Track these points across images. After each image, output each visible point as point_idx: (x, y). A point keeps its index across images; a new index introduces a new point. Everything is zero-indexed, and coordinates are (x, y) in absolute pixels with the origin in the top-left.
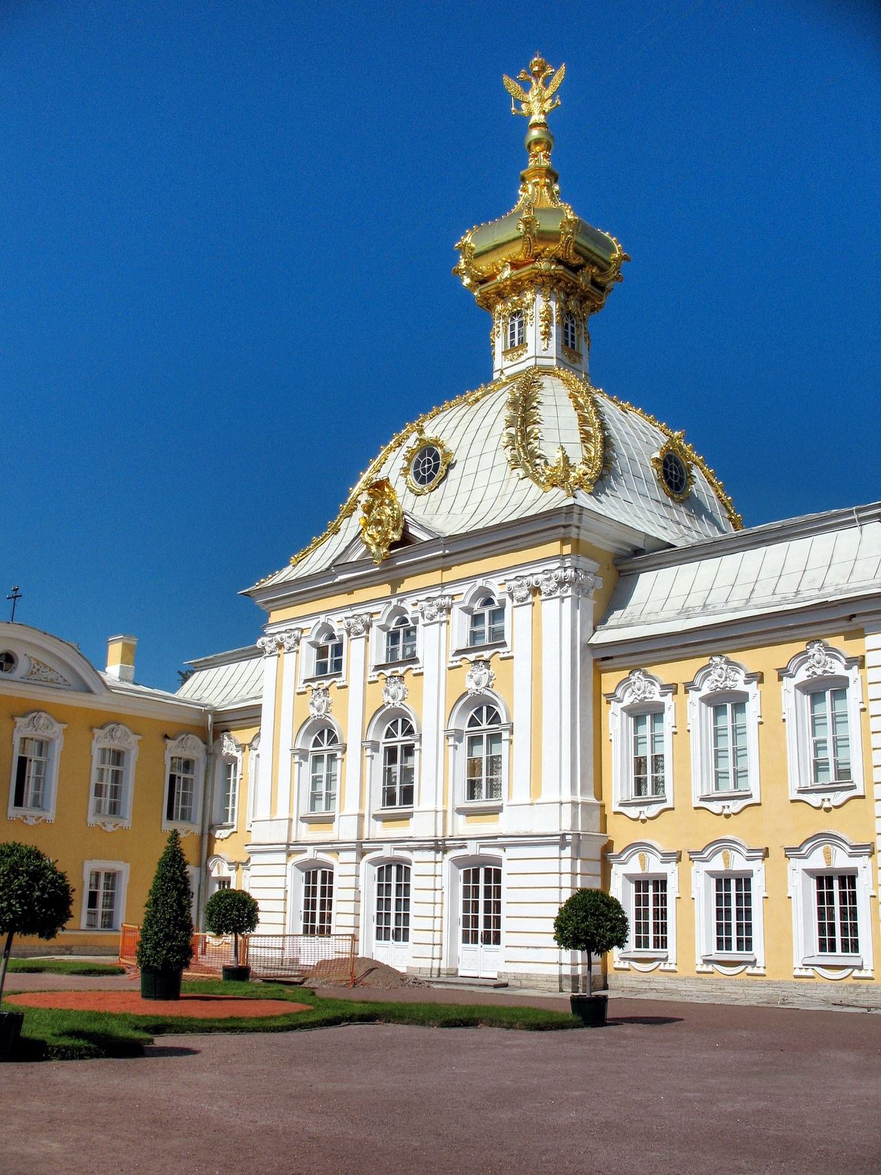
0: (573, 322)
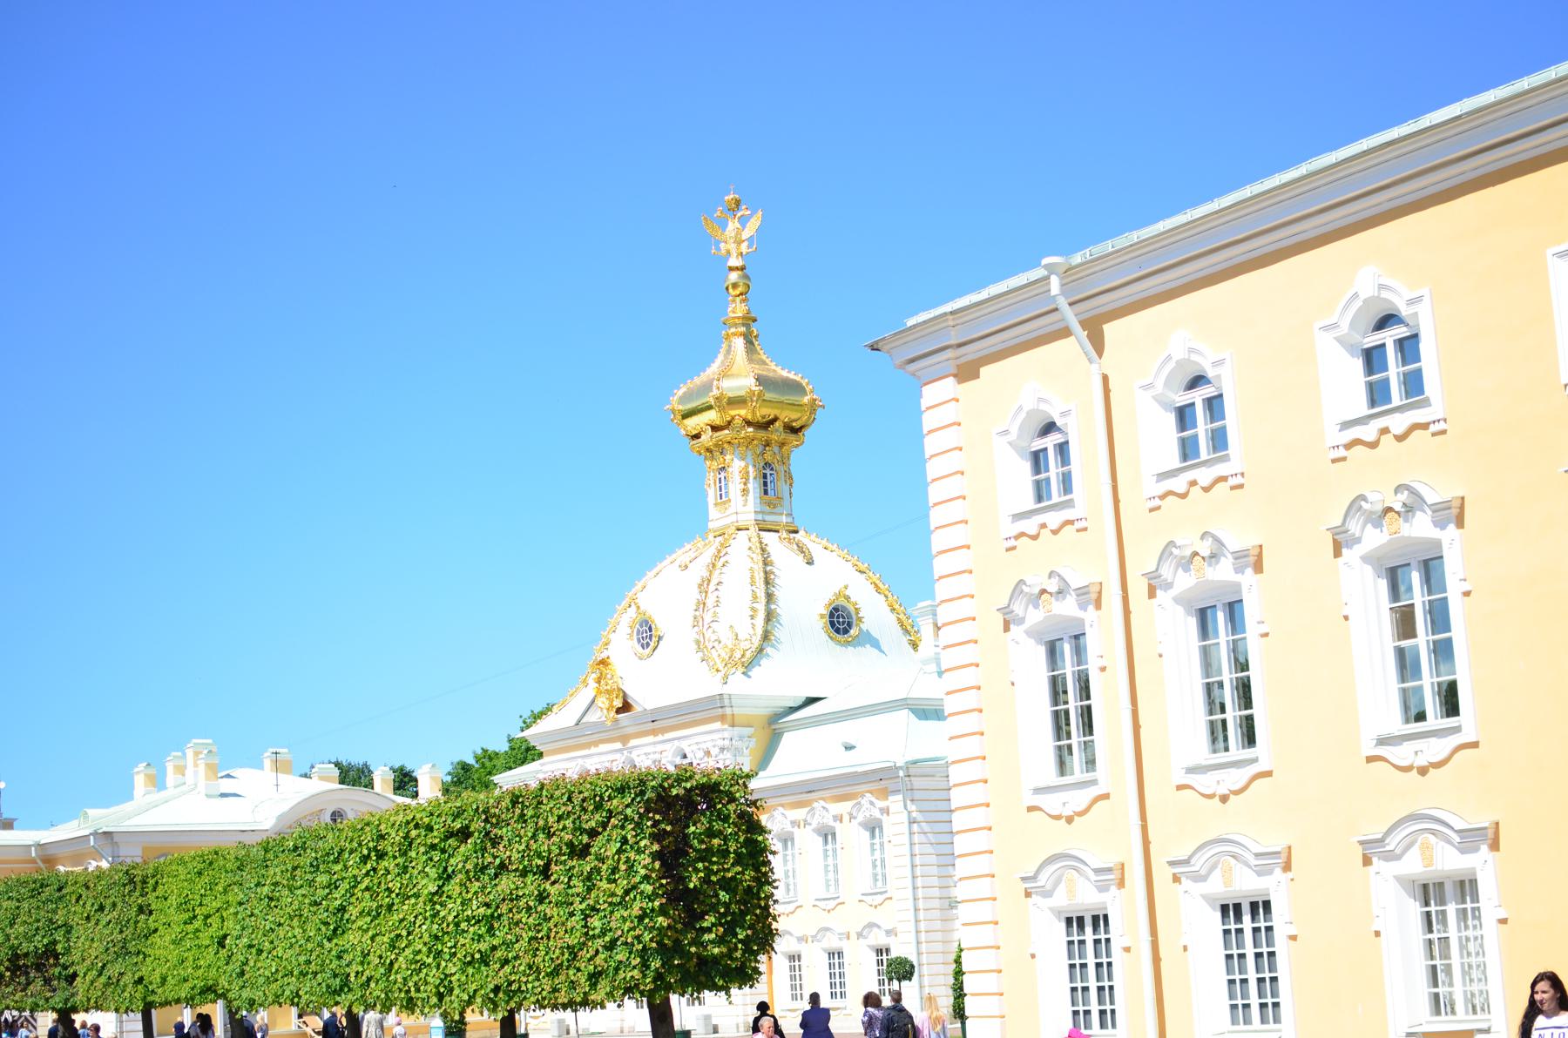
0: (772, 469)
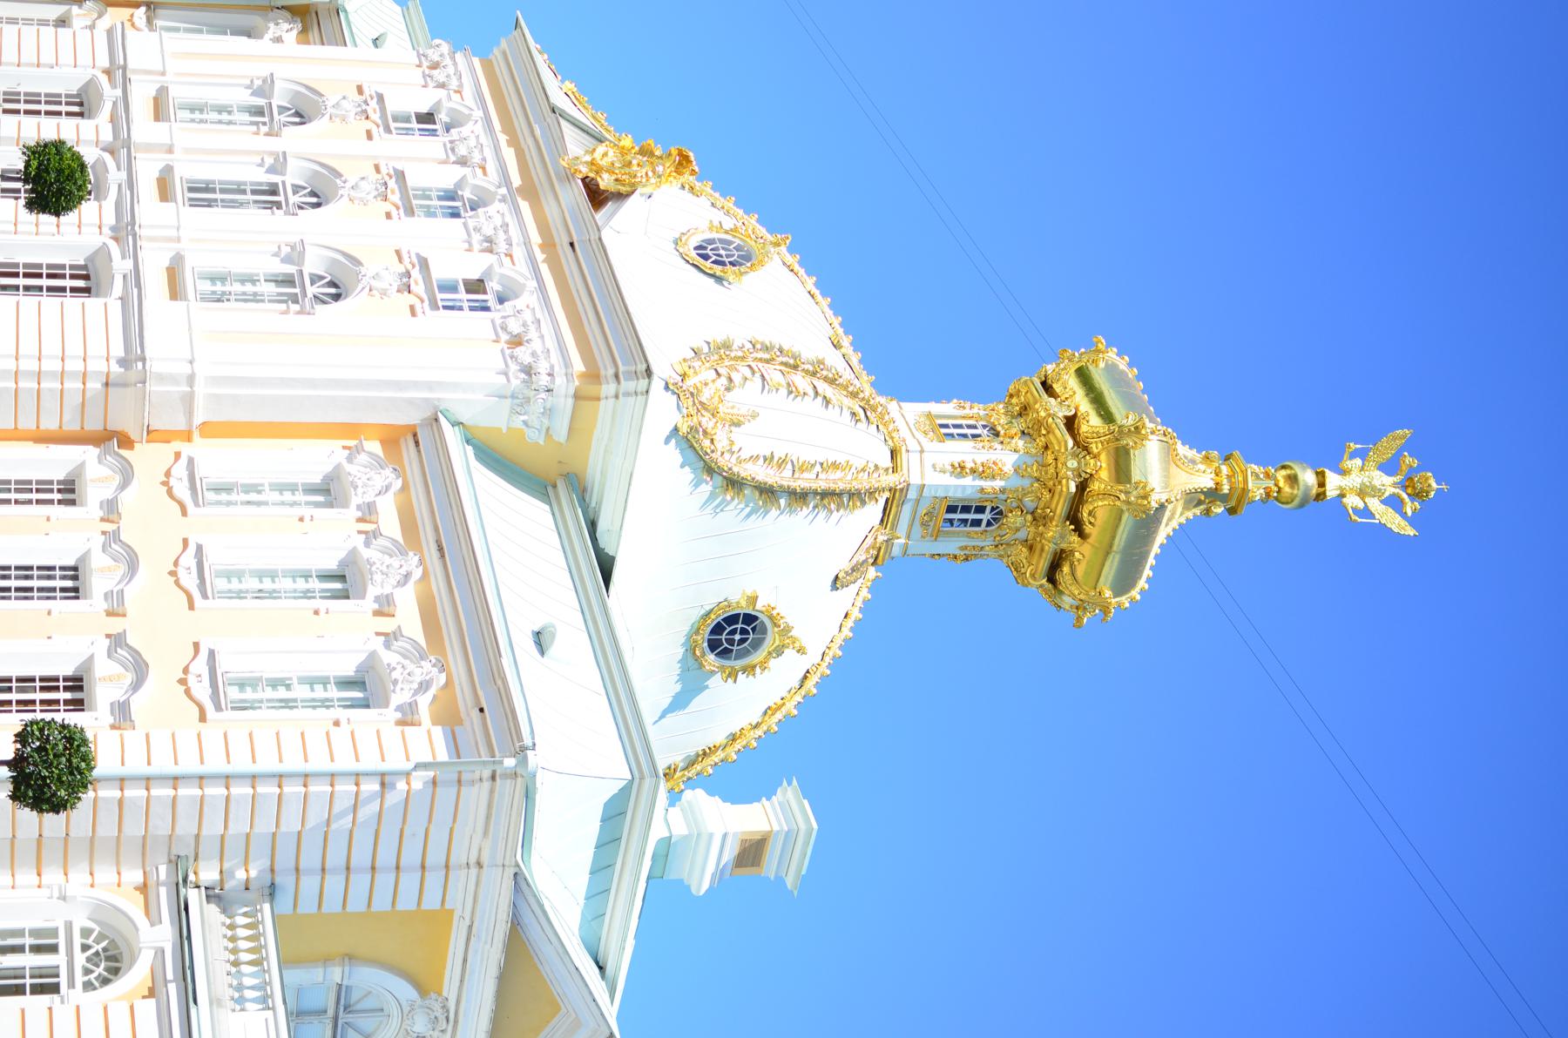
0: (989, 524)
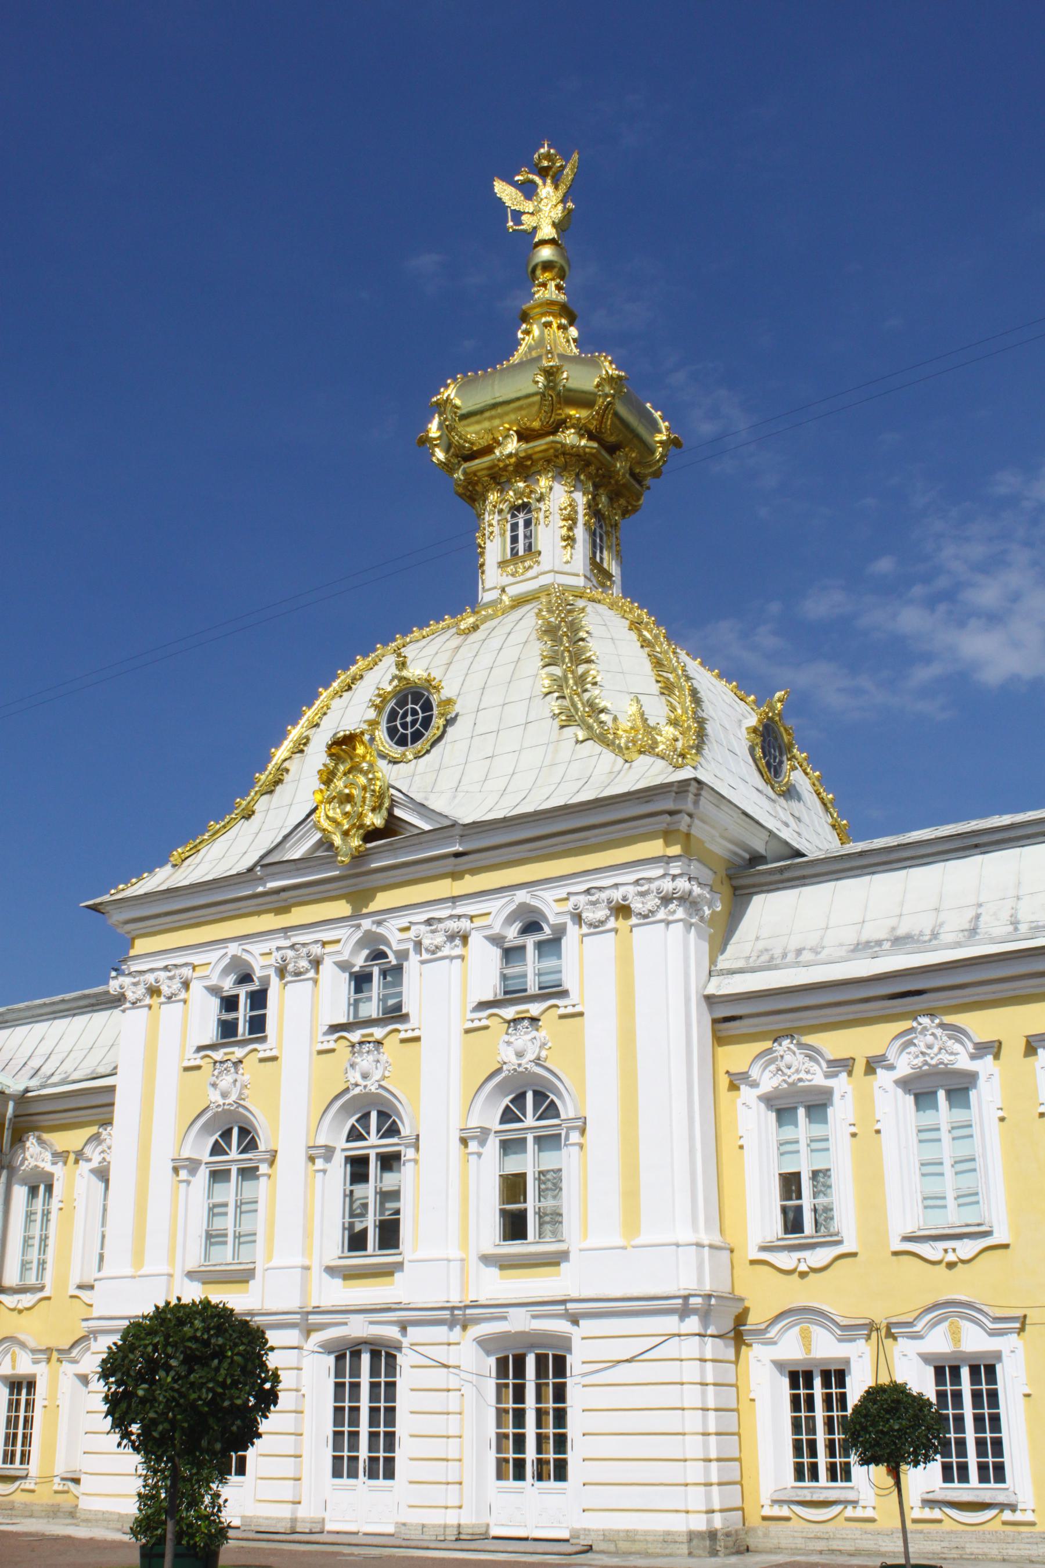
0: (601, 527)
